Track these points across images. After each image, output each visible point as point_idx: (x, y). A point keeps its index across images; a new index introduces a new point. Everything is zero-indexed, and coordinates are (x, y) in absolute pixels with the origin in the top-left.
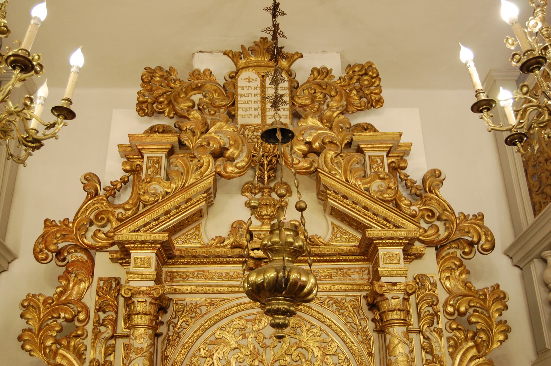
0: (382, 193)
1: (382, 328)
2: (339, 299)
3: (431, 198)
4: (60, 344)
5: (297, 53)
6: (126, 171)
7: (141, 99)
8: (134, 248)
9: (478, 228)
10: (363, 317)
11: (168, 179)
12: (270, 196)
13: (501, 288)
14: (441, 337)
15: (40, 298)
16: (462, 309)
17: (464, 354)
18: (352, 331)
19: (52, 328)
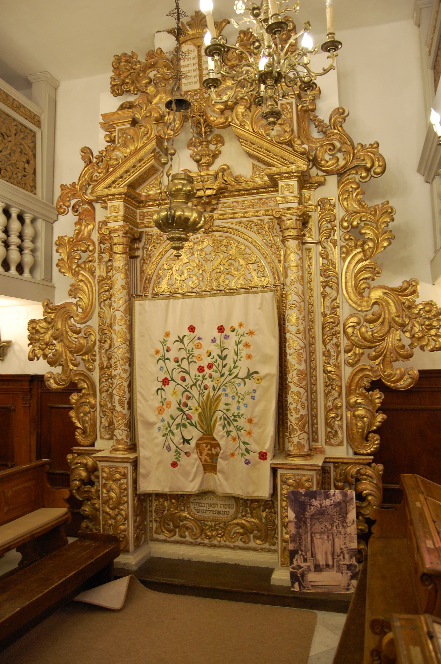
0: (279, 136)
2: (259, 222)
3: (334, 134)
4: (80, 267)
5: (225, 20)
6: (107, 141)
7: (113, 83)
8: (109, 200)
9: (372, 155)
10: (276, 234)
12: (208, 148)
13: (390, 204)
14: (335, 246)
15: (66, 238)
16: (355, 223)
17: (352, 258)
18: (267, 246)
19: (74, 258)
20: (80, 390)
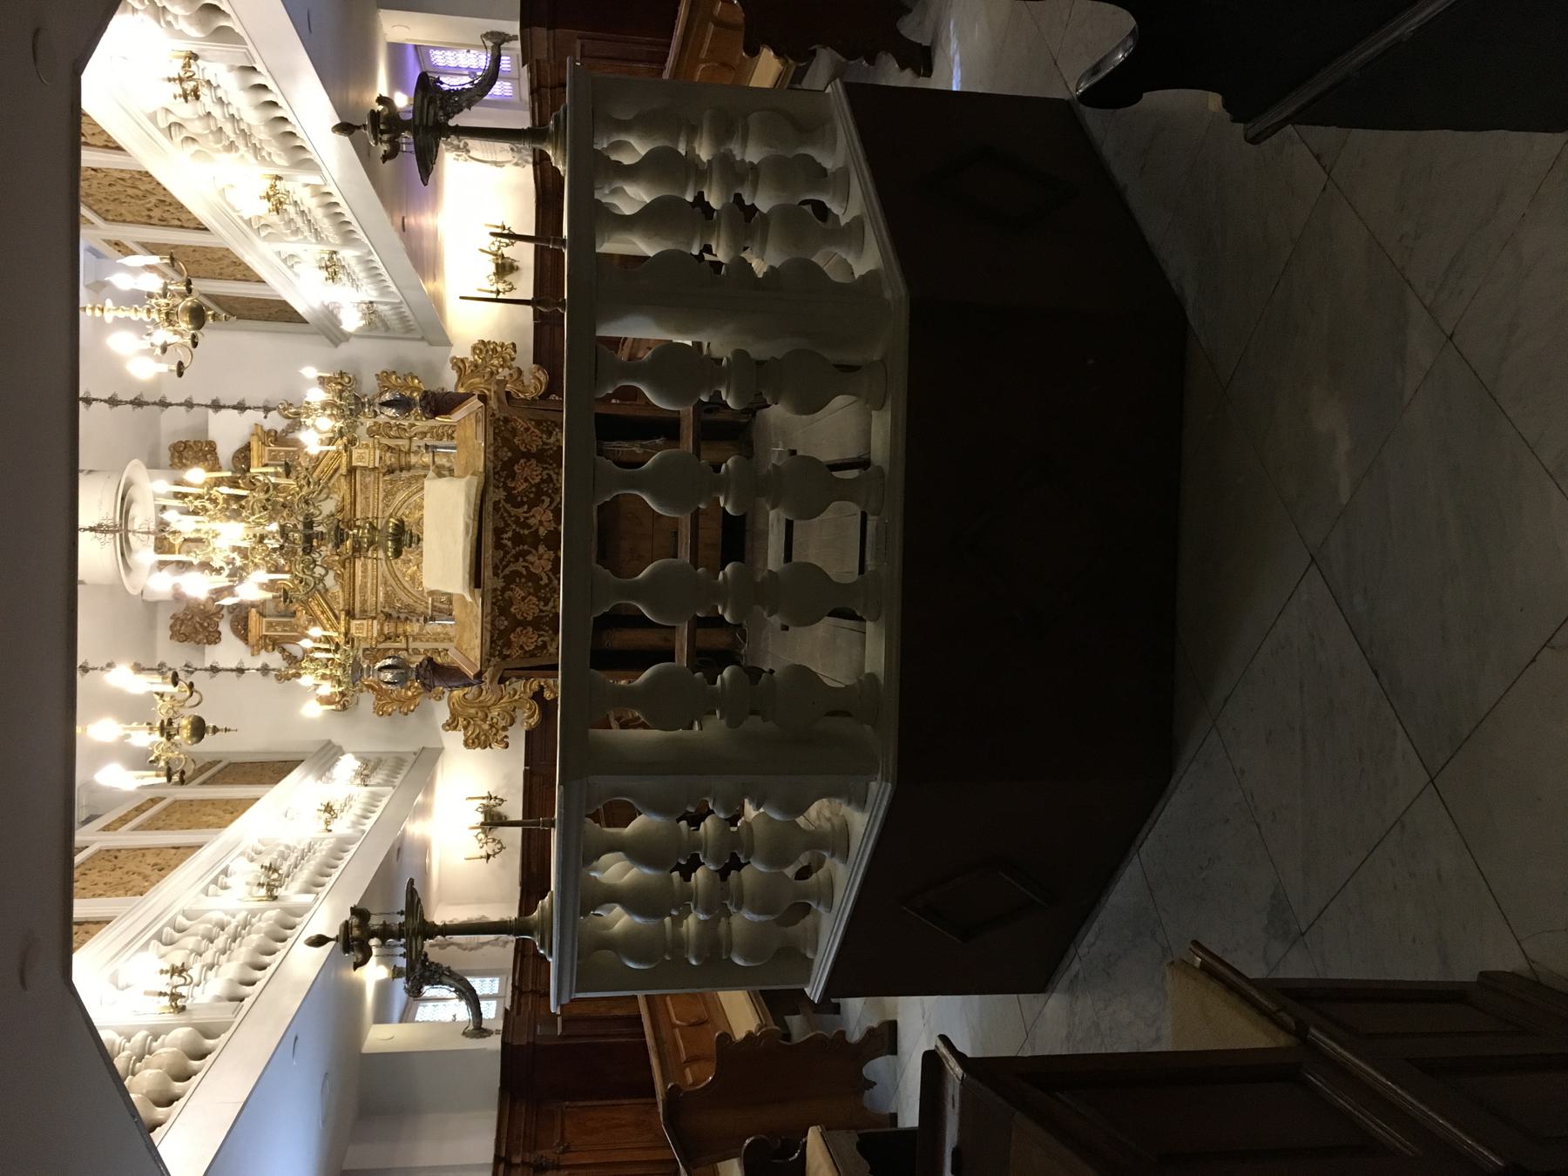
1: (409, 467)
11: (294, 614)
20: (542, 688)
